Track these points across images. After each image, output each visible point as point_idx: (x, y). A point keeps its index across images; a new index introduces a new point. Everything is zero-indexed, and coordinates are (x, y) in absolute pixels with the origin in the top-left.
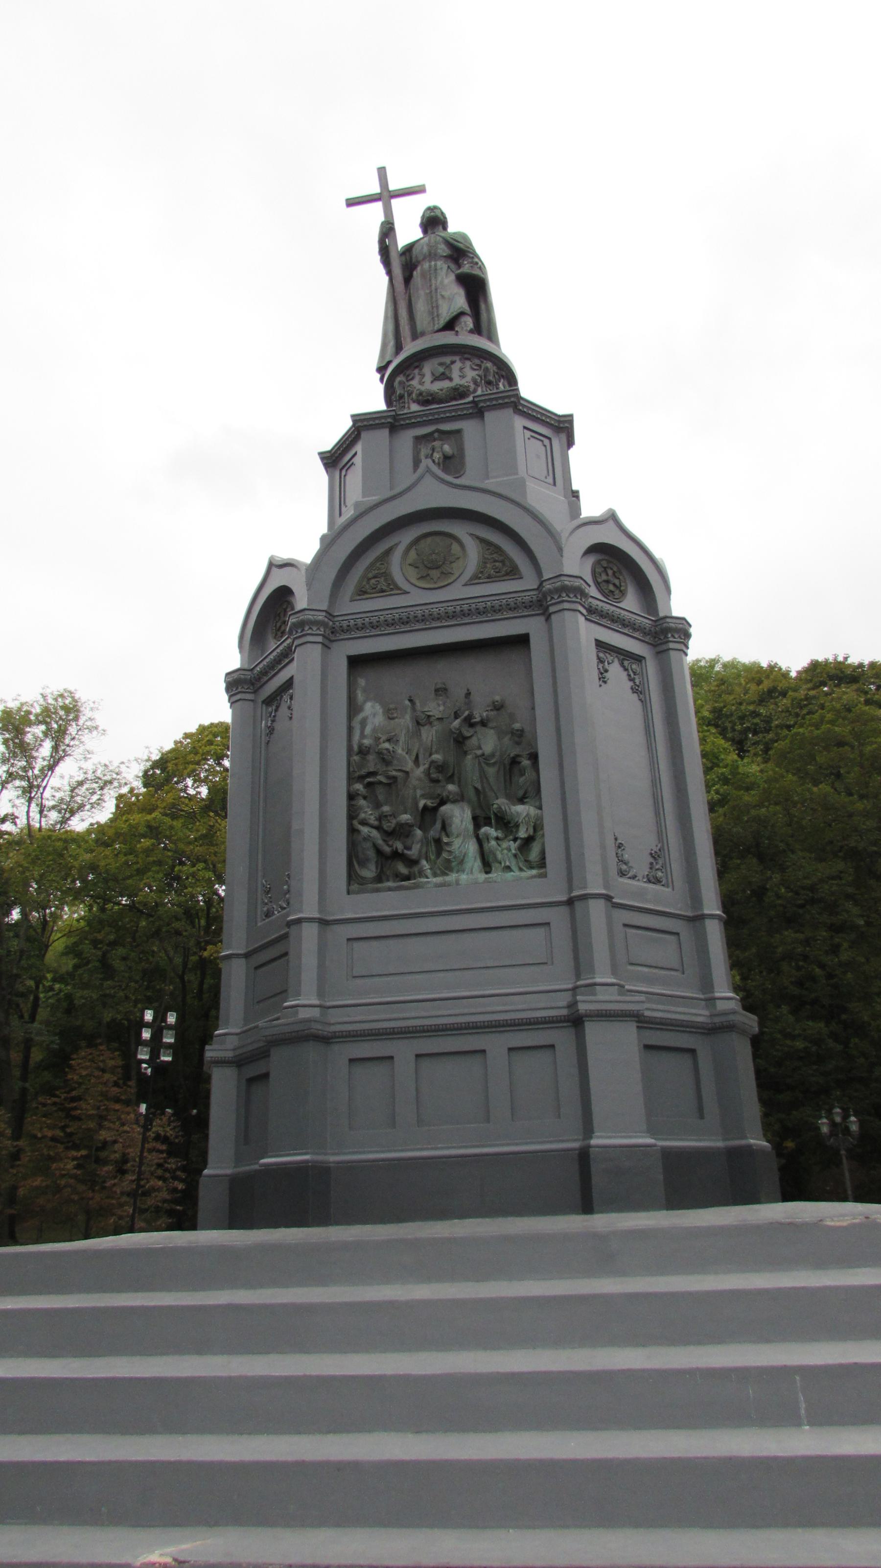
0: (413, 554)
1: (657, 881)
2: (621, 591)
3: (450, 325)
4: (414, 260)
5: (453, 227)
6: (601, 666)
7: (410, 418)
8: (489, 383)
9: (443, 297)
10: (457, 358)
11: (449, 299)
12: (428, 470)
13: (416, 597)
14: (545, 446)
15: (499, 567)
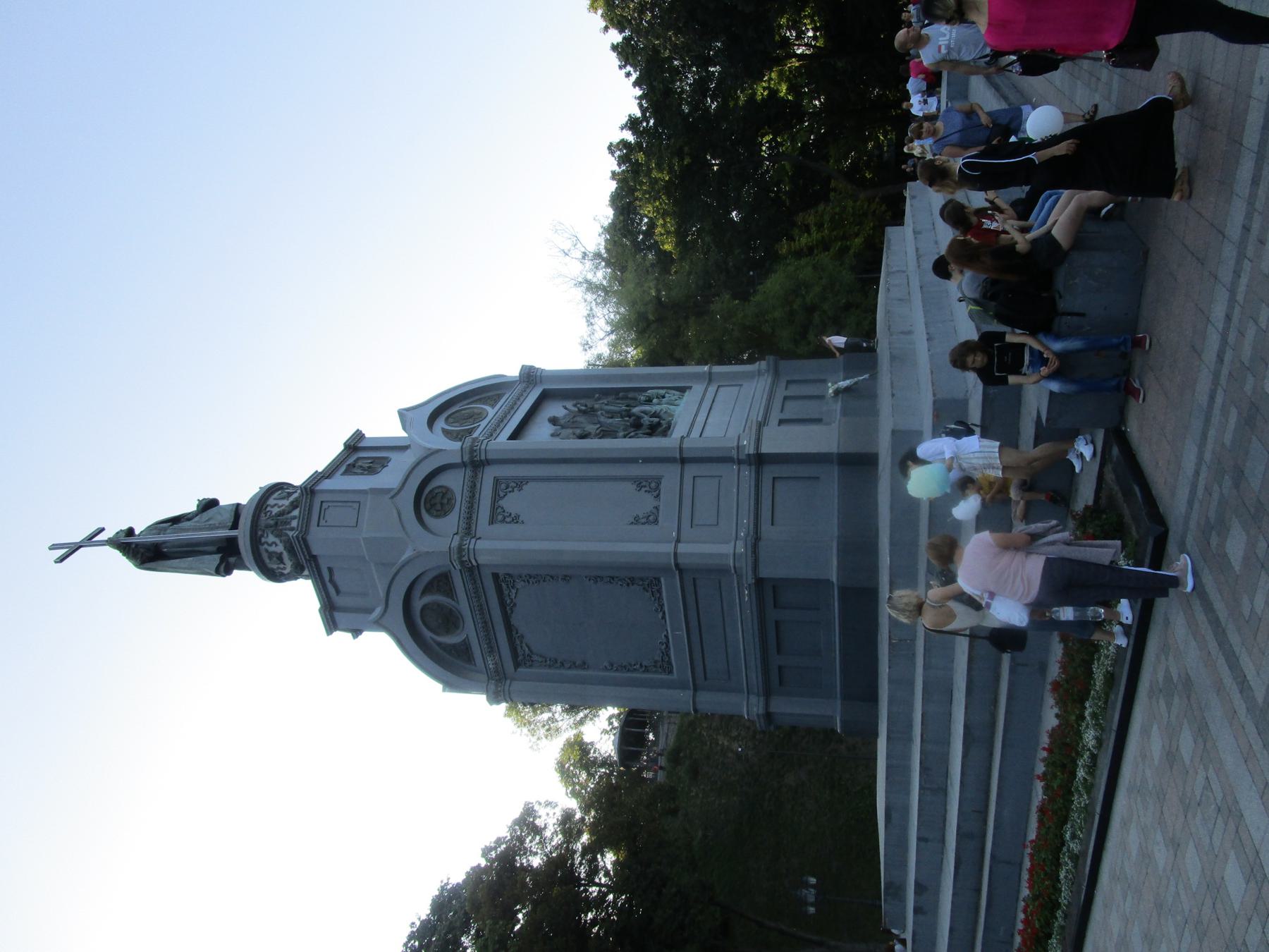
1: (658, 488)
6: (508, 520)
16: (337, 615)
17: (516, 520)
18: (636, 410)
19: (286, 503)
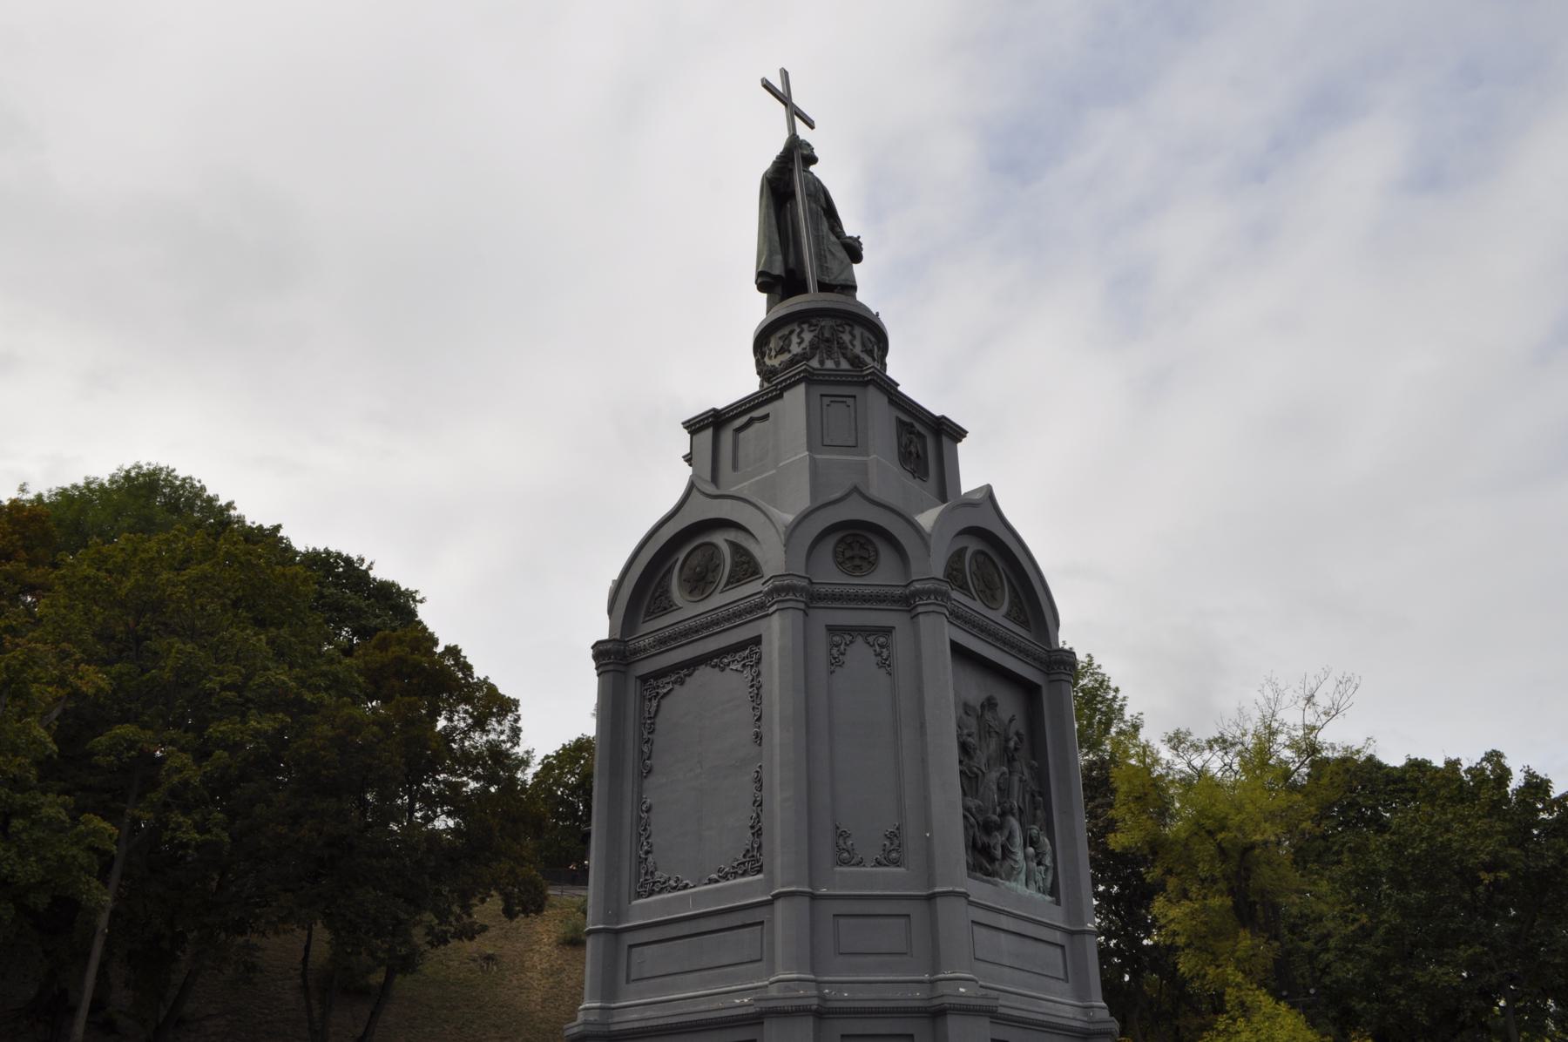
6: (835, 651)
16: (708, 434)
17: (835, 662)
18: (1014, 823)
19: (858, 350)
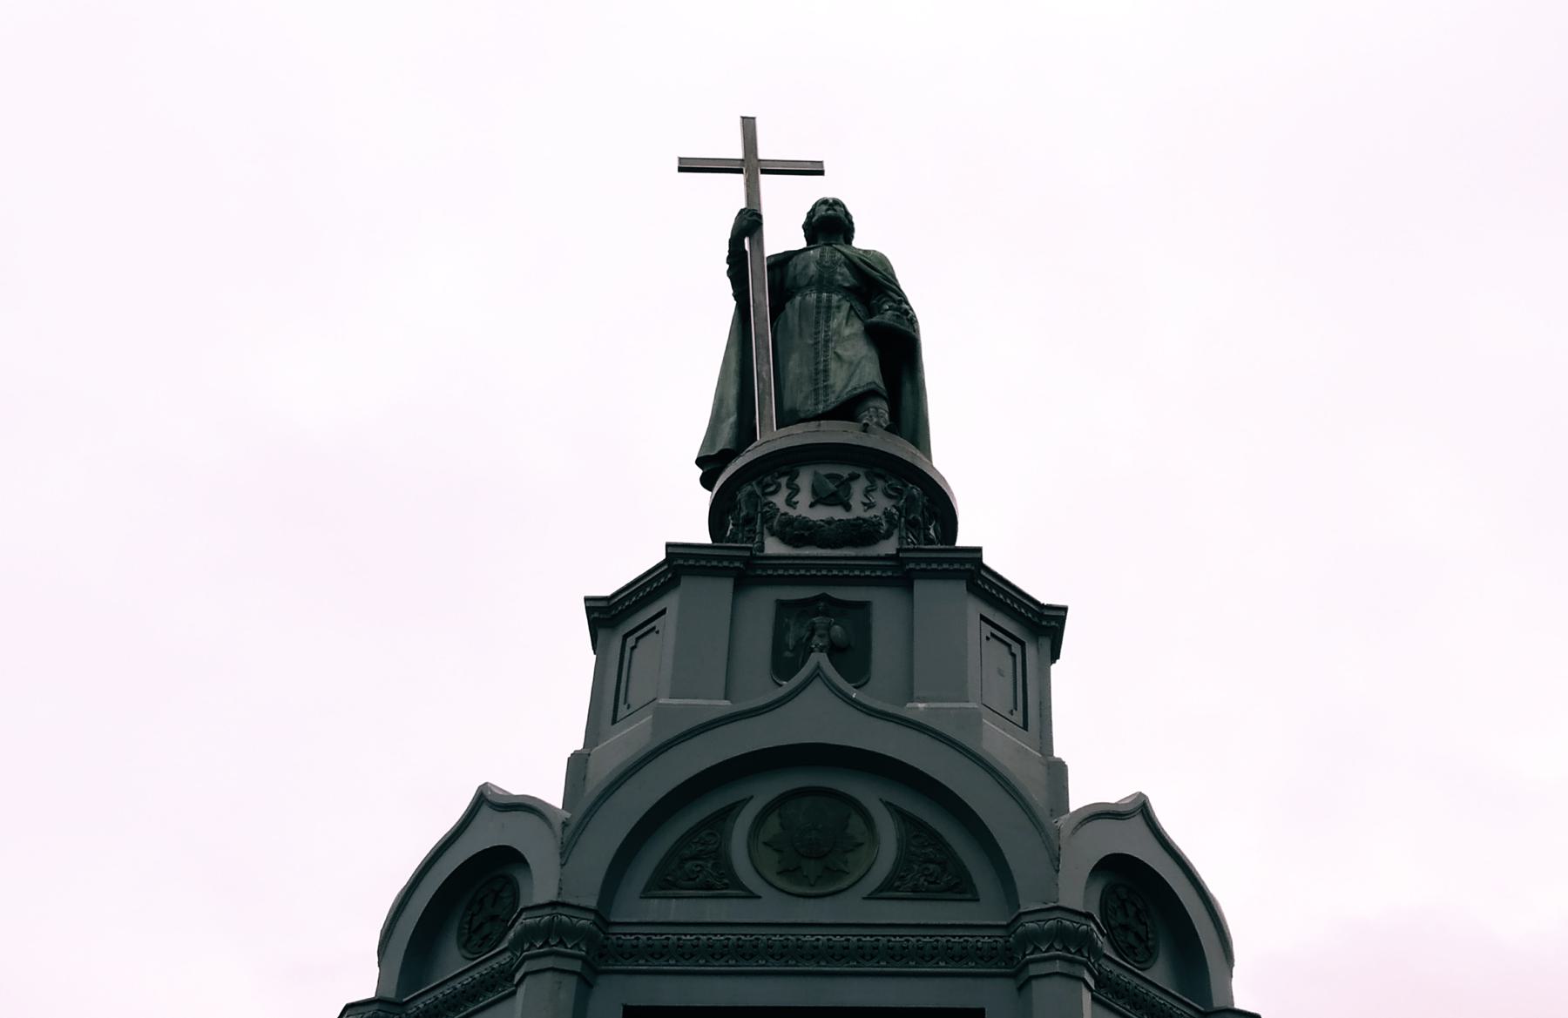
0: (773, 825)
2: (1147, 948)
3: (847, 410)
4: (788, 283)
5: (862, 240)
7: (775, 567)
8: (912, 525)
9: (839, 357)
10: (861, 471)
11: (851, 363)
12: (817, 673)
13: (771, 908)
14: (1013, 655)
15: (931, 869)
